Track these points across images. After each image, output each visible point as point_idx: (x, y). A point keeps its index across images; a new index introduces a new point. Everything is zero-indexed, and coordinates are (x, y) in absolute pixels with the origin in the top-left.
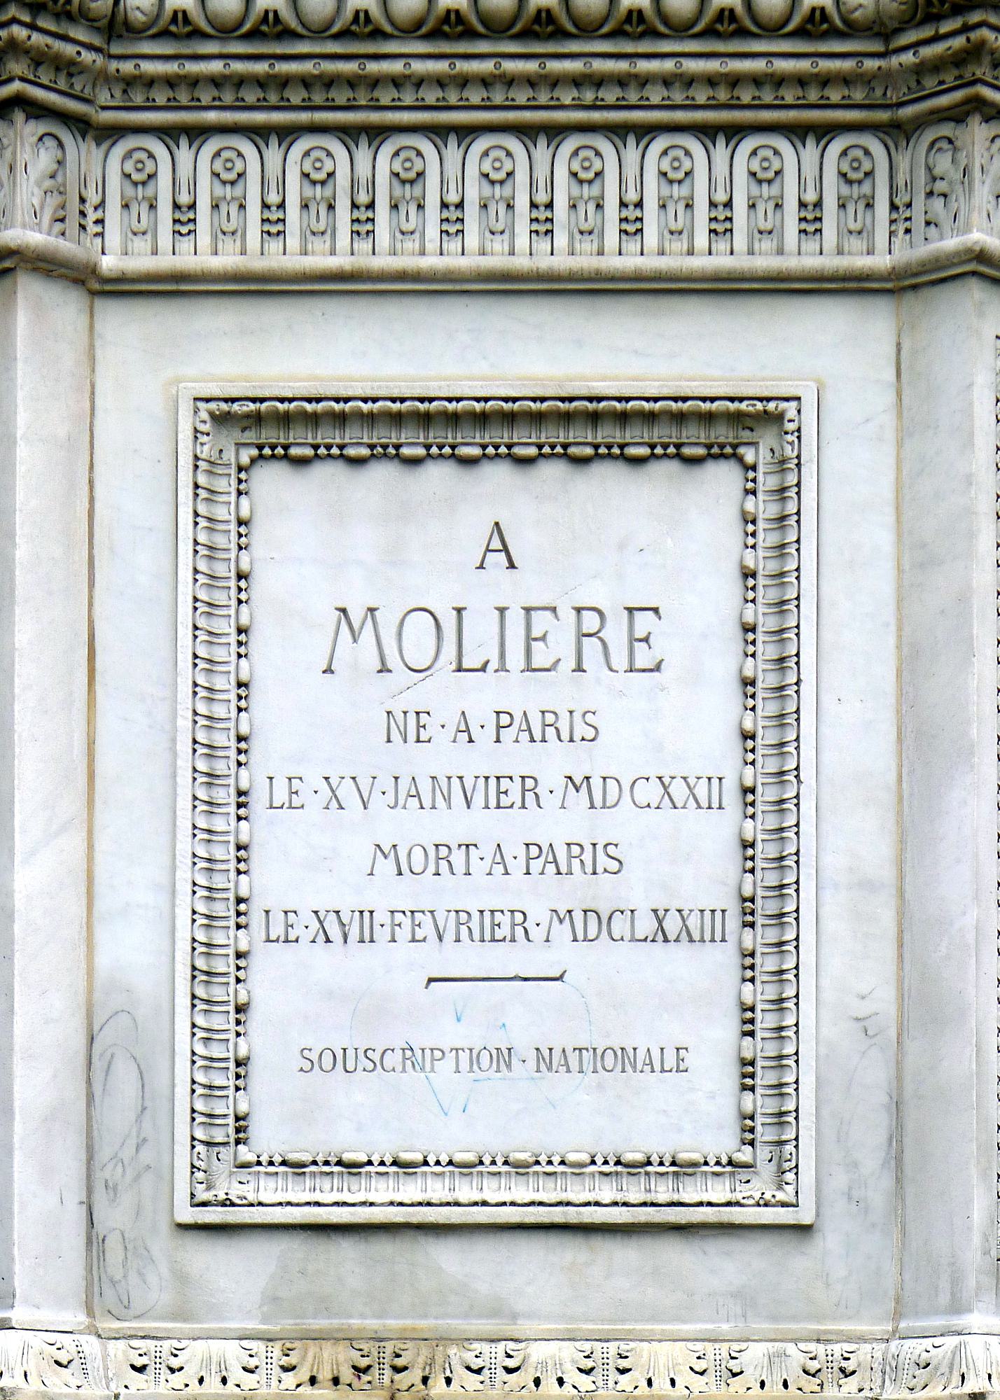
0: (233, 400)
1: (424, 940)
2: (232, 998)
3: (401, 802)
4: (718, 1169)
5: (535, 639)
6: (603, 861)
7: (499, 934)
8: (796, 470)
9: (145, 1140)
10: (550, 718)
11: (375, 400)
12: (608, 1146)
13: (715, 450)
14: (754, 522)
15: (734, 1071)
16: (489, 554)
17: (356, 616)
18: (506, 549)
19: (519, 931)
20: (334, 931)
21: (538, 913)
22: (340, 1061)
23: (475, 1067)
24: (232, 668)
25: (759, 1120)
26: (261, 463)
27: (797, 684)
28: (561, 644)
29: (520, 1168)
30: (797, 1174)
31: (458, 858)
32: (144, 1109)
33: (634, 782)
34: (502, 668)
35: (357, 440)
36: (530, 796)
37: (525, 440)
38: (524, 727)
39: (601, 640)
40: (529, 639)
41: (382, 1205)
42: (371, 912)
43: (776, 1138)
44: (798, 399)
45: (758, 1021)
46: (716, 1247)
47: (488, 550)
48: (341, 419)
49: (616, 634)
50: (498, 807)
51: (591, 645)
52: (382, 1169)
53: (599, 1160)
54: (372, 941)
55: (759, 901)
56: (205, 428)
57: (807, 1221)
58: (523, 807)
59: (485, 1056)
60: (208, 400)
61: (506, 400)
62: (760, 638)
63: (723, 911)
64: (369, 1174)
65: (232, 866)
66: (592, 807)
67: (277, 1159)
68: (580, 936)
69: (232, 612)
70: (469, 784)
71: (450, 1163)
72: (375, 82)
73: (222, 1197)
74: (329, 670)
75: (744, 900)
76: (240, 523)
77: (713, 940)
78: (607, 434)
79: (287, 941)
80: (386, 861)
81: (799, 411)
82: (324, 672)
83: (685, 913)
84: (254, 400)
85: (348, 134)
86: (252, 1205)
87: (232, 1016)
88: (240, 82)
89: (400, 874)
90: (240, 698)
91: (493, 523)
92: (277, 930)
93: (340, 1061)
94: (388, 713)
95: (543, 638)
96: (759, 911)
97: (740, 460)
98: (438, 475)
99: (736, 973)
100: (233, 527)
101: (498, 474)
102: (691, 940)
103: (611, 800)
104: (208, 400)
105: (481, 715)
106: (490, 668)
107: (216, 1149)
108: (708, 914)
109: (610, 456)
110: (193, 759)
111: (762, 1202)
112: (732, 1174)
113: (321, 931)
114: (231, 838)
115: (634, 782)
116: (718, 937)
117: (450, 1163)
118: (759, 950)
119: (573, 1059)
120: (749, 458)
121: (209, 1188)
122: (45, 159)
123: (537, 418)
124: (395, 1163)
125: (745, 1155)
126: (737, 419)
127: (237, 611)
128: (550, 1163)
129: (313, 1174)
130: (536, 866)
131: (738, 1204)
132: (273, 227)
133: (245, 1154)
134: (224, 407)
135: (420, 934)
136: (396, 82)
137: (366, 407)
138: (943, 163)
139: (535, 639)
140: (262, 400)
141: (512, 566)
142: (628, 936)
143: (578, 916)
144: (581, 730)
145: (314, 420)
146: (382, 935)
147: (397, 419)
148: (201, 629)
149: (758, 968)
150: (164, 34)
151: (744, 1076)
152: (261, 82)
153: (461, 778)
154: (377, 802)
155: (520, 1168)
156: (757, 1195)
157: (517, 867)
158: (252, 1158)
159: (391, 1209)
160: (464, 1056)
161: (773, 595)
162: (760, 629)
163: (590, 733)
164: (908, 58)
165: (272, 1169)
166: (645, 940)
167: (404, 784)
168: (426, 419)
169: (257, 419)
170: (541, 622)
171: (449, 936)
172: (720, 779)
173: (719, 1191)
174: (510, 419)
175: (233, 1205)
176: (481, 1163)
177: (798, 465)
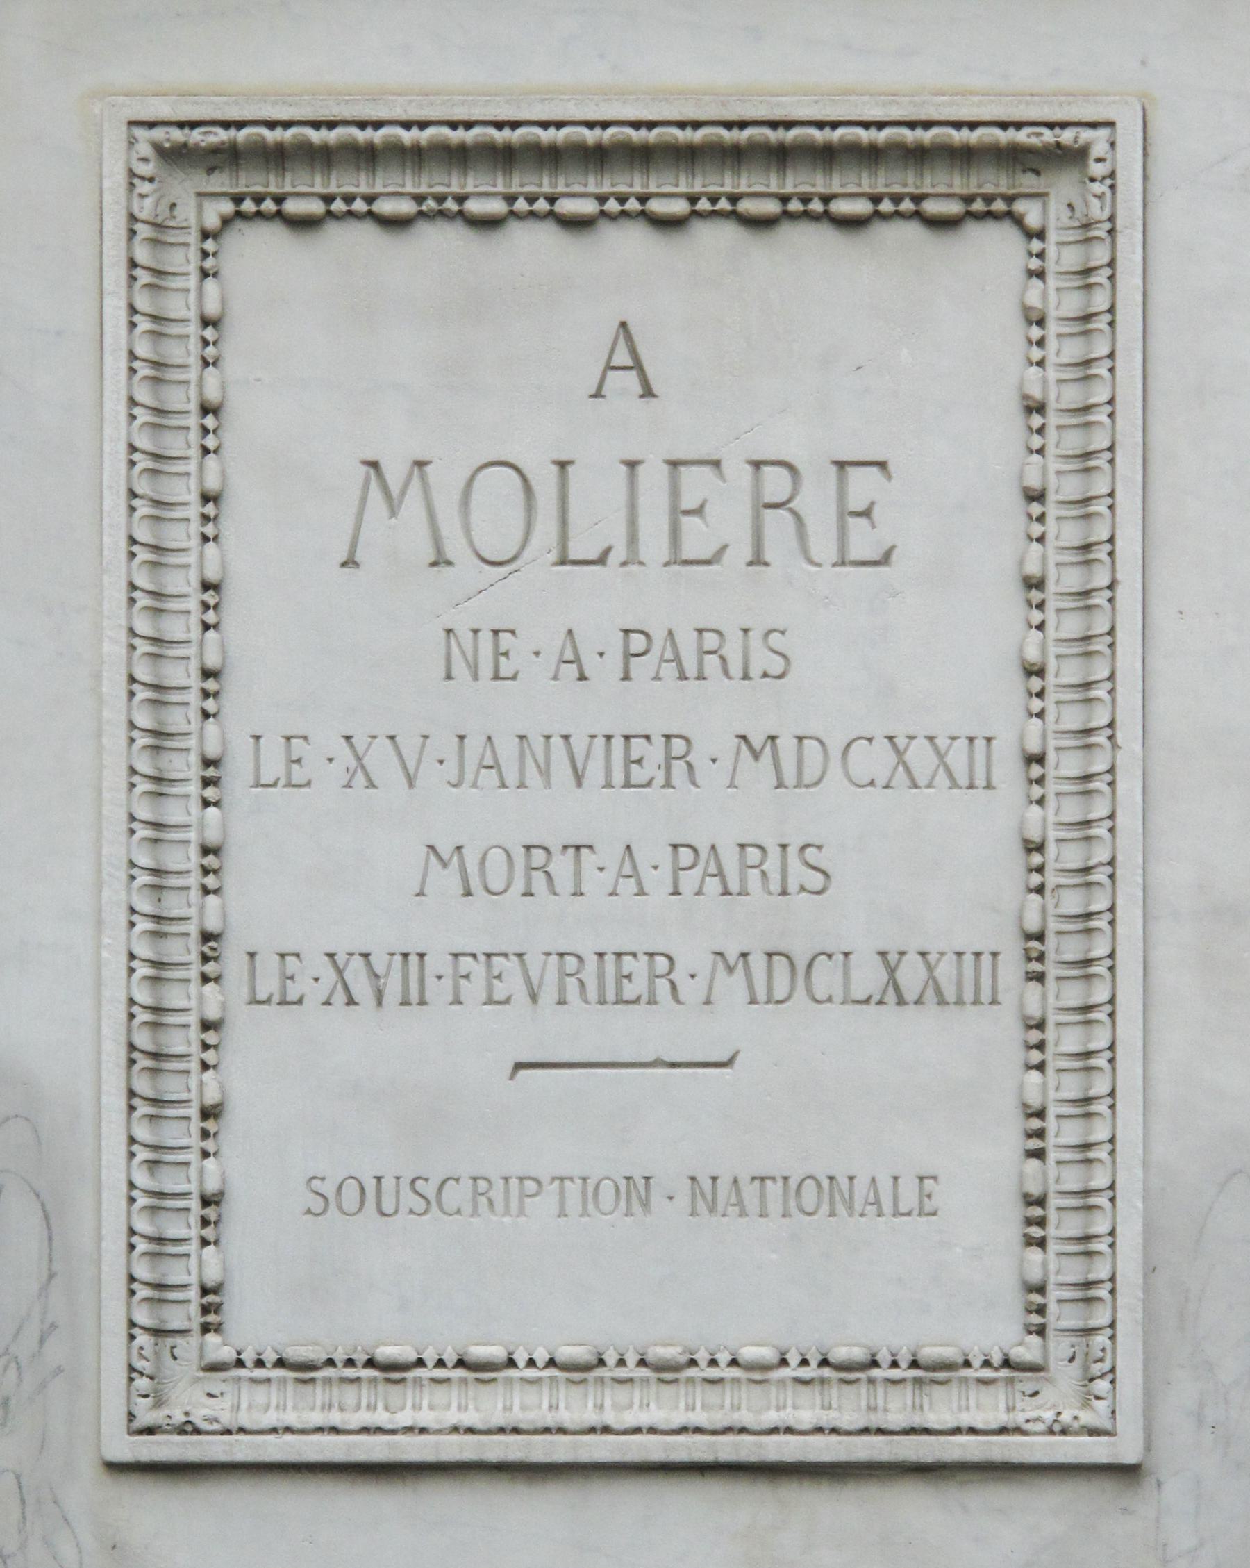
0: (193, 125)
1: (507, 1001)
2: (194, 1095)
3: (469, 776)
4: (987, 1373)
5: (687, 513)
7: (630, 991)
8: (1108, 240)
9: (53, 1326)
10: (711, 640)
11: (423, 125)
13: (978, 206)
14: (1041, 323)
15: (1014, 1213)
16: (611, 374)
17: (395, 473)
18: (638, 366)
19: (663, 986)
20: (361, 987)
23: (591, 1207)
24: (192, 559)
25: (1053, 1294)
26: (239, 225)
27: (1111, 587)
29: (666, 1371)
30: (1113, 1382)
31: (562, 866)
32: (51, 1276)
33: (849, 745)
36: (679, 768)
38: (669, 655)
39: (793, 512)
40: (677, 512)
41: (439, 1432)
42: (421, 956)
43: (1079, 1324)
44: (1111, 124)
45: (1050, 1134)
47: (609, 367)
48: (368, 156)
50: (628, 785)
51: (777, 525)
52: (440, 1373)
53: (794, 1359)
54: (422, 1002)
55: (1051, 939)
56: (144, 169)
57: (1130, 1458)
58: (668, 784)
59: (607, 1188)
60: (152, 125)
61: (636, 125)
62: (1052, 511)
63: (995, 955)
64: (418, 1382)
65: (194, 880)
66: (780, 785)
67: (270, 1357)
68: (761, 994)
69: (192, 467)
70: (579, 745)
71: (551, 1363)
73: (179, 1418)
74: (350, 562)
75: (1029, 937)
76: (206, 322)
77: (976, 1002)
79: (283, 1002)
80: (446, 872)
81: (1113, 144)
82: (344, 565)
83: (932, 958)
84: (226, 125)
86: (228, 1432)
87: (196, 1124)
89: (468, 893)
90: (206, 606)
91: (617, 324)
92: (268, 985)
94: (449, 631)
95: (699, 511)
96: (1051, 956)
97: (1018, 221)
99: (1017, 1055)
100: (193, 329)
102: (942, 1002)
103: (810, 775)
104: (152, 125)
106: (614, 558)
107: (170, 1341)
108: (968, 959)
109: (807, 215)
110: (129, 709)
111: (1057, 1428)
112: (1010, 1381)
113: (339, 986)
114: (192, 835)
115: (849, 745)
116: (986, 995)
117: (551, 1363)
118: (1052, 1019)
119: (750, 1192)
120: (1033, 219)
121: (159, 1403)
123: (688, 156)
124: (461, 1363)
125: (1029, 1350)
126: (1014, 157)
127: (201, 467)
128: (713, 1363)
129: (328, 1381)
130: (689, 880)
131: (1018, 1430)
133: (218, 1348)
134: (177, 135)
135: (500, 991)
137: (407, 137)
139: (687, 513)
140: (240, 125)
141: (648, 392)
142: (838, 995)
143: (758, 963)
144: (762, 660)
145: (323, 157)
146: (439, 992)
147: (459, 156)
148: (142, 497)
149: (1050, 1048)
151: (1029, 1222)
153: (566, 738)
154: (430, 776)
155: (666, 1371)
156: (1049, 1415)
158: (227, 1354)
159: (455, 1438)
160: (573, 1189)
161: (1074, 441)
162: (1051, 497)
163: (777, 665)
165: (260, 1373)
166: (867, 1001)
167: (474, 745)
168: (505, 157)
169: (230, 157)
170: (696, 484)
171: (548, 995)
172: (989, 740)
174: (642, 156)
175: (197, 1431)
176: (601, 1362)
177: (1111, 232)
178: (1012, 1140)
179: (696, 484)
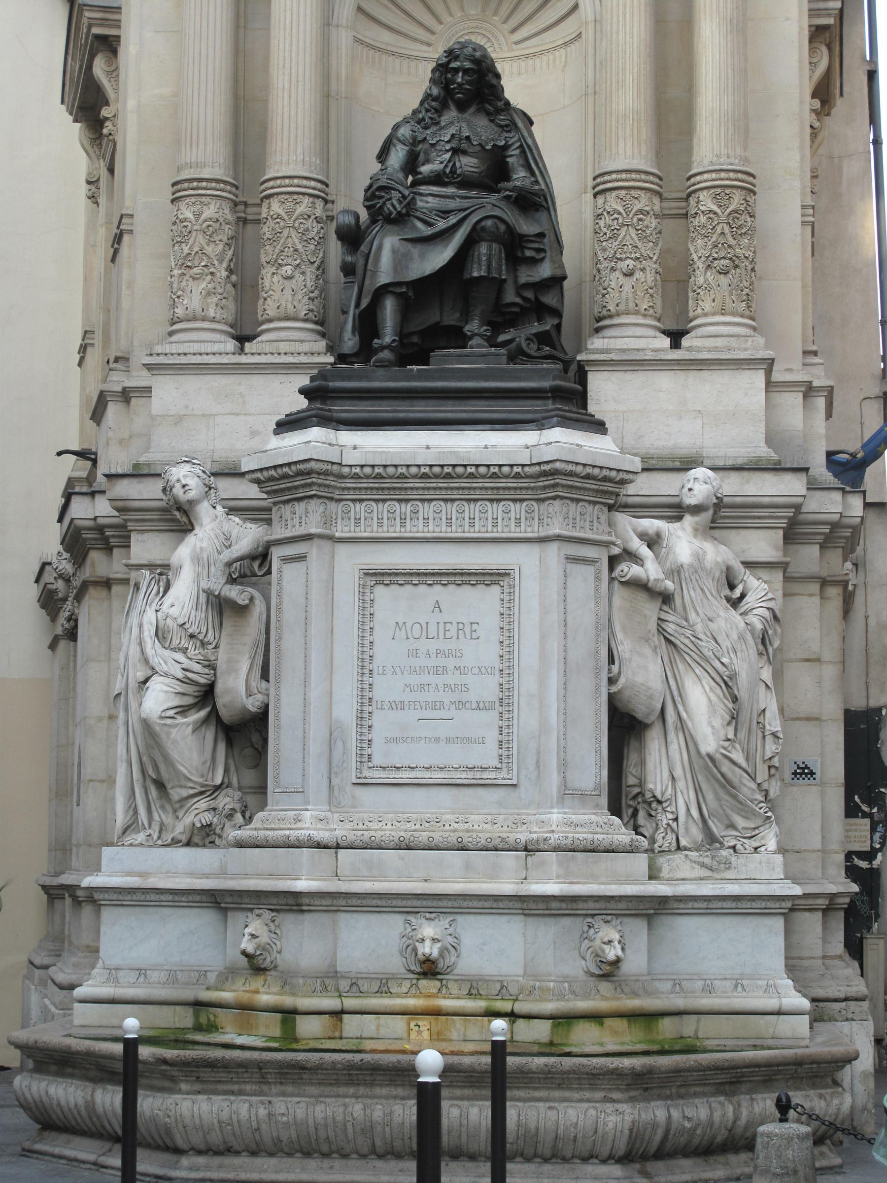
6: (464, 689)
12: (464, 764)
20: (394, 707)
21: (447, 702)
22: (395, 740)
28: (453, 632)
29: (441, 769)
31: (426, 688)
34: (438, 638)
35: (401, 579)
37: (444, 580)
40: (445, 631)
46: (491, 790)
48: (397, 574)
49: (467, 629)
57: (515, 783)
72: (406, 489)
78: (465, 578)
85: (400, 501)
88: (372, 488)
93: (395, 740)
98: (423, 588)
99: (498, 718)
101: (438, 588)
105: (433, 651)
122: (322, 509)
125: (499, 766)
126: (499, 574)
132: (380, 524)
133: (370, 765)
136: (412, 489)
138: (551, 510)
144: (458, 654)
146: (406, 707)
147: (411, 574)
150: (352, 477)
152: (377, 489)
154: (405, 673)
155: (441, 769)
157: (441, 690)
161: (508, 620)
164: (541, 484)
168: (418, 574)
173: (492, 775)
174: (440, 574)
178: (497, 732)
179: (448, 626)
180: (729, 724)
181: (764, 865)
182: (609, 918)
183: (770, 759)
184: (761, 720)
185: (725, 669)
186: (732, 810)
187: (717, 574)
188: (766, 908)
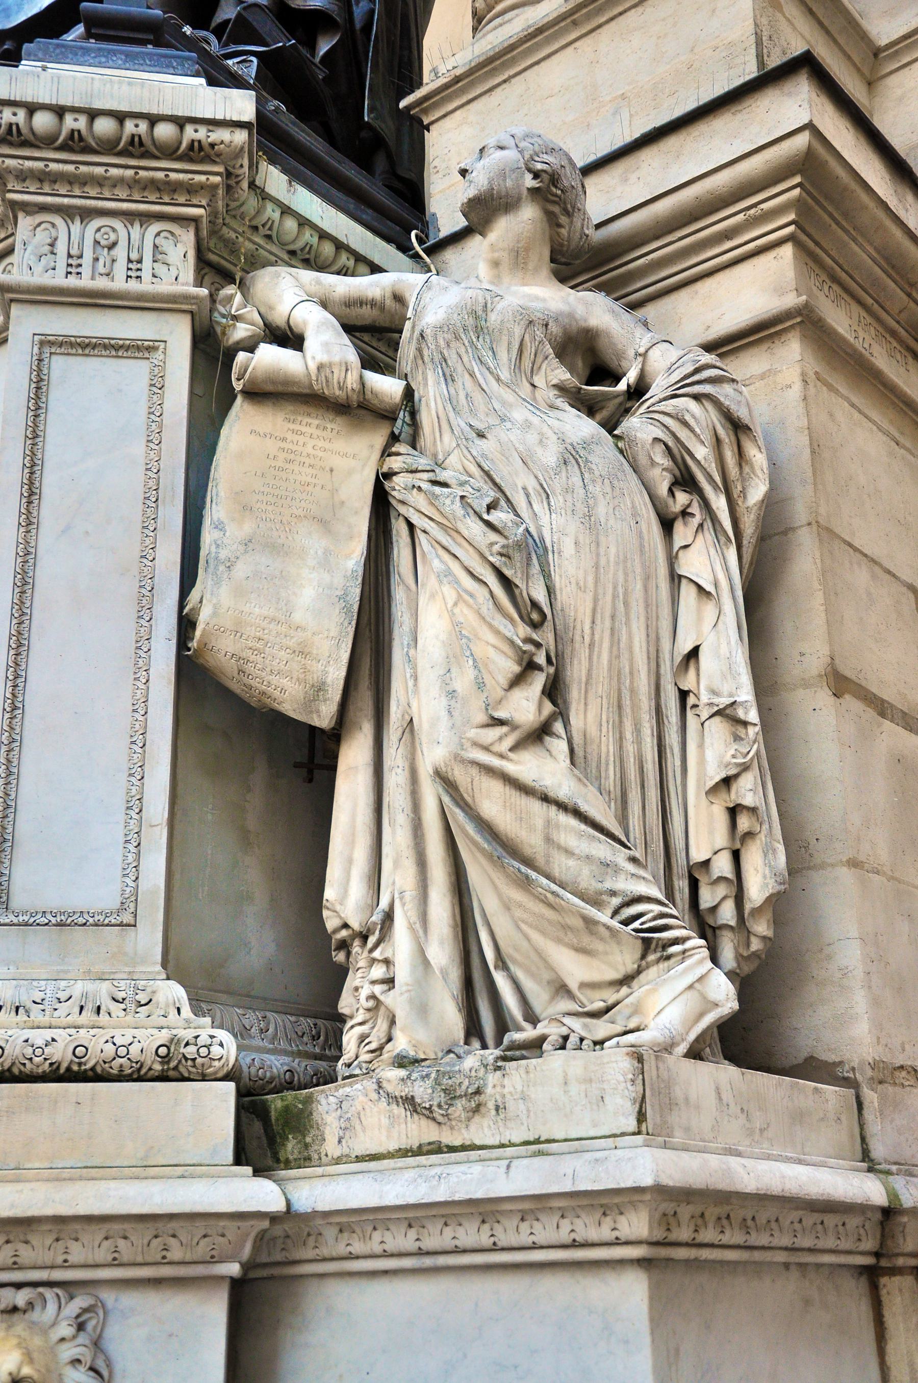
180: (517, 681)
181: (574, 1089)
182: (21, 1298)
183: (727, 782)
184: (688, 683)
185: (493, 537)
186: (543, 933)
187: (518, 331)
188: (575, 1245)
